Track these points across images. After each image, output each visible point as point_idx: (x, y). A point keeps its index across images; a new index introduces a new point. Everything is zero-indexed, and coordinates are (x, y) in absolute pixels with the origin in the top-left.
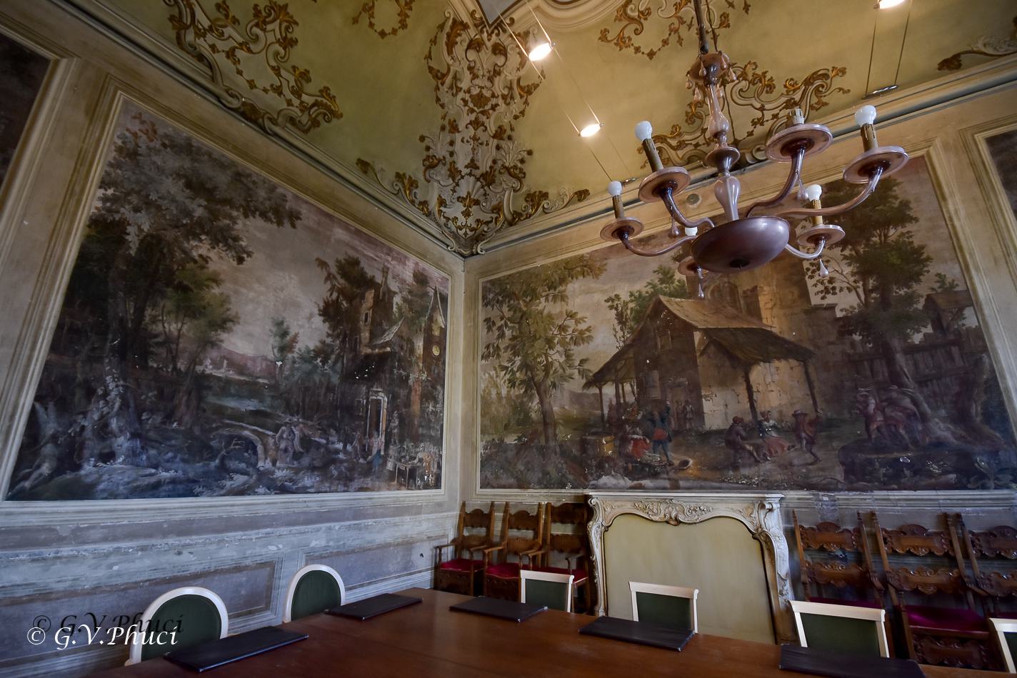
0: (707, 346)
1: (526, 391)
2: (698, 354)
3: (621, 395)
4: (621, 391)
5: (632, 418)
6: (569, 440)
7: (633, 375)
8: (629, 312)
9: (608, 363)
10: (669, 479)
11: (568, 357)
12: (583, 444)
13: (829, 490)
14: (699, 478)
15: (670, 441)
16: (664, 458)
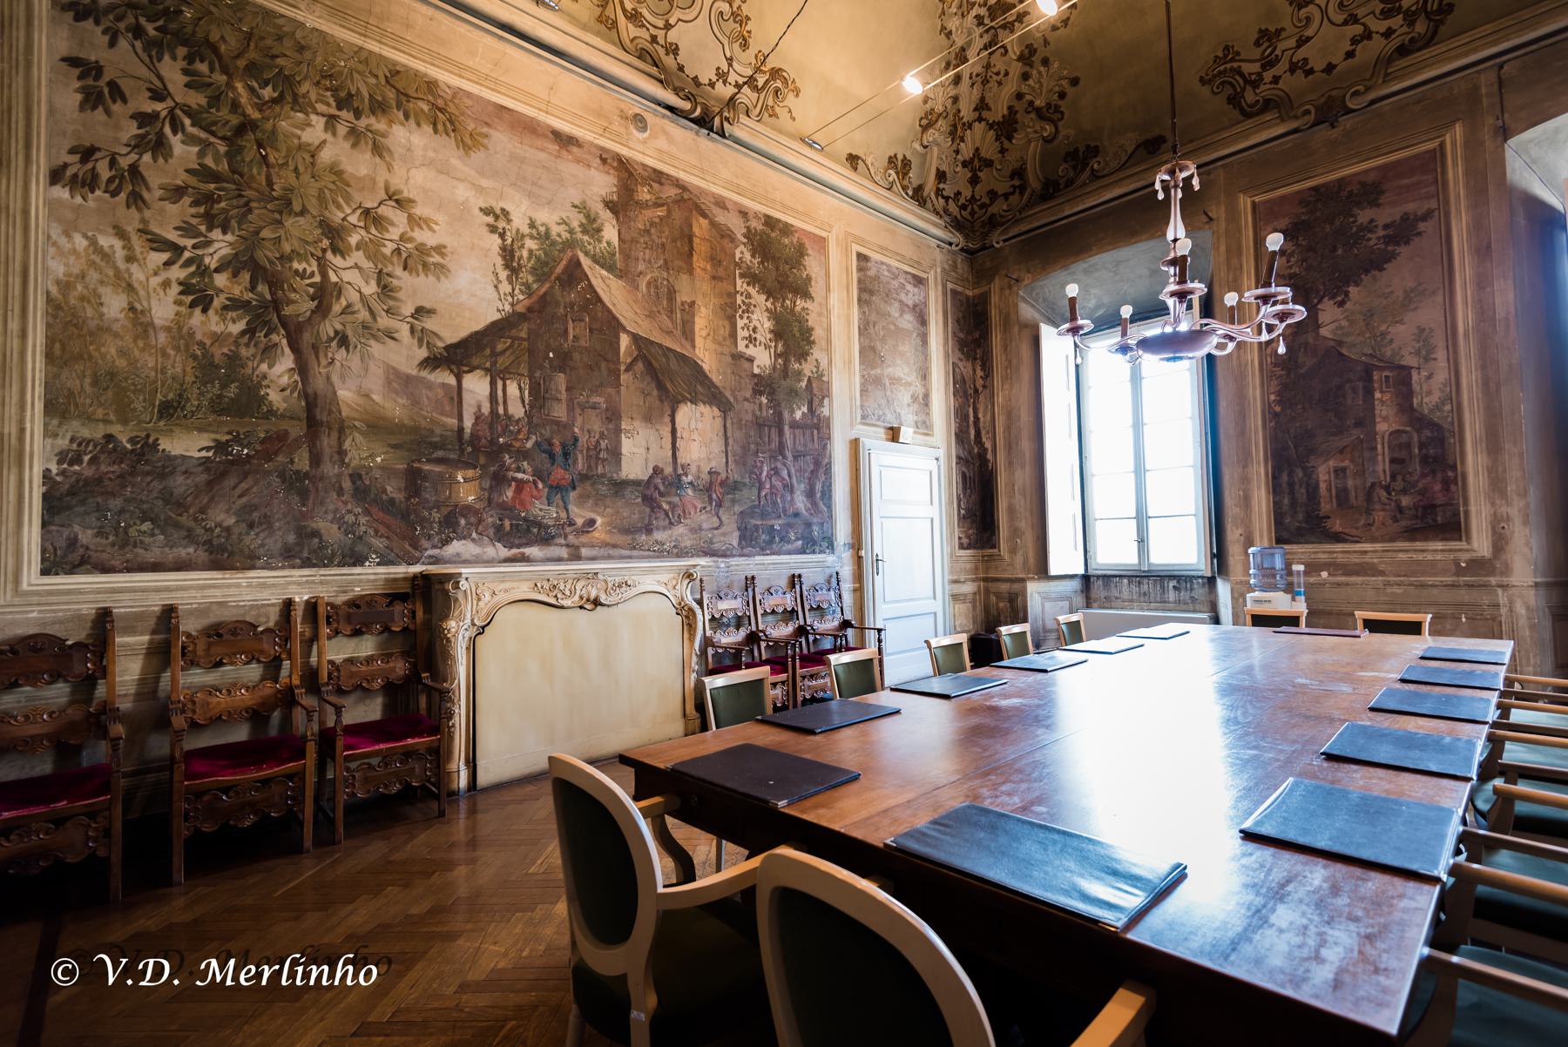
0: (635, 360)
1: (250, 331)
2: (623, 368)
3: (500, 400)
4: (500, 393)
5: (517, 444)
6: (382, 468)
7: (524, 369)
8: (525, 254)
9: (476, 333)
10: (567, 546)
11: (386, 290)
12: (414, 480)
13: (725, 556)
14: (605, 545)
15: (574, 488)
16: (563, 515)
